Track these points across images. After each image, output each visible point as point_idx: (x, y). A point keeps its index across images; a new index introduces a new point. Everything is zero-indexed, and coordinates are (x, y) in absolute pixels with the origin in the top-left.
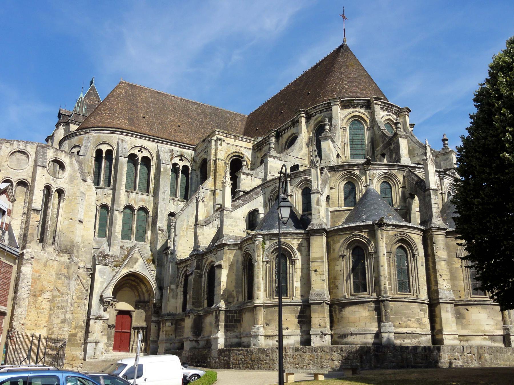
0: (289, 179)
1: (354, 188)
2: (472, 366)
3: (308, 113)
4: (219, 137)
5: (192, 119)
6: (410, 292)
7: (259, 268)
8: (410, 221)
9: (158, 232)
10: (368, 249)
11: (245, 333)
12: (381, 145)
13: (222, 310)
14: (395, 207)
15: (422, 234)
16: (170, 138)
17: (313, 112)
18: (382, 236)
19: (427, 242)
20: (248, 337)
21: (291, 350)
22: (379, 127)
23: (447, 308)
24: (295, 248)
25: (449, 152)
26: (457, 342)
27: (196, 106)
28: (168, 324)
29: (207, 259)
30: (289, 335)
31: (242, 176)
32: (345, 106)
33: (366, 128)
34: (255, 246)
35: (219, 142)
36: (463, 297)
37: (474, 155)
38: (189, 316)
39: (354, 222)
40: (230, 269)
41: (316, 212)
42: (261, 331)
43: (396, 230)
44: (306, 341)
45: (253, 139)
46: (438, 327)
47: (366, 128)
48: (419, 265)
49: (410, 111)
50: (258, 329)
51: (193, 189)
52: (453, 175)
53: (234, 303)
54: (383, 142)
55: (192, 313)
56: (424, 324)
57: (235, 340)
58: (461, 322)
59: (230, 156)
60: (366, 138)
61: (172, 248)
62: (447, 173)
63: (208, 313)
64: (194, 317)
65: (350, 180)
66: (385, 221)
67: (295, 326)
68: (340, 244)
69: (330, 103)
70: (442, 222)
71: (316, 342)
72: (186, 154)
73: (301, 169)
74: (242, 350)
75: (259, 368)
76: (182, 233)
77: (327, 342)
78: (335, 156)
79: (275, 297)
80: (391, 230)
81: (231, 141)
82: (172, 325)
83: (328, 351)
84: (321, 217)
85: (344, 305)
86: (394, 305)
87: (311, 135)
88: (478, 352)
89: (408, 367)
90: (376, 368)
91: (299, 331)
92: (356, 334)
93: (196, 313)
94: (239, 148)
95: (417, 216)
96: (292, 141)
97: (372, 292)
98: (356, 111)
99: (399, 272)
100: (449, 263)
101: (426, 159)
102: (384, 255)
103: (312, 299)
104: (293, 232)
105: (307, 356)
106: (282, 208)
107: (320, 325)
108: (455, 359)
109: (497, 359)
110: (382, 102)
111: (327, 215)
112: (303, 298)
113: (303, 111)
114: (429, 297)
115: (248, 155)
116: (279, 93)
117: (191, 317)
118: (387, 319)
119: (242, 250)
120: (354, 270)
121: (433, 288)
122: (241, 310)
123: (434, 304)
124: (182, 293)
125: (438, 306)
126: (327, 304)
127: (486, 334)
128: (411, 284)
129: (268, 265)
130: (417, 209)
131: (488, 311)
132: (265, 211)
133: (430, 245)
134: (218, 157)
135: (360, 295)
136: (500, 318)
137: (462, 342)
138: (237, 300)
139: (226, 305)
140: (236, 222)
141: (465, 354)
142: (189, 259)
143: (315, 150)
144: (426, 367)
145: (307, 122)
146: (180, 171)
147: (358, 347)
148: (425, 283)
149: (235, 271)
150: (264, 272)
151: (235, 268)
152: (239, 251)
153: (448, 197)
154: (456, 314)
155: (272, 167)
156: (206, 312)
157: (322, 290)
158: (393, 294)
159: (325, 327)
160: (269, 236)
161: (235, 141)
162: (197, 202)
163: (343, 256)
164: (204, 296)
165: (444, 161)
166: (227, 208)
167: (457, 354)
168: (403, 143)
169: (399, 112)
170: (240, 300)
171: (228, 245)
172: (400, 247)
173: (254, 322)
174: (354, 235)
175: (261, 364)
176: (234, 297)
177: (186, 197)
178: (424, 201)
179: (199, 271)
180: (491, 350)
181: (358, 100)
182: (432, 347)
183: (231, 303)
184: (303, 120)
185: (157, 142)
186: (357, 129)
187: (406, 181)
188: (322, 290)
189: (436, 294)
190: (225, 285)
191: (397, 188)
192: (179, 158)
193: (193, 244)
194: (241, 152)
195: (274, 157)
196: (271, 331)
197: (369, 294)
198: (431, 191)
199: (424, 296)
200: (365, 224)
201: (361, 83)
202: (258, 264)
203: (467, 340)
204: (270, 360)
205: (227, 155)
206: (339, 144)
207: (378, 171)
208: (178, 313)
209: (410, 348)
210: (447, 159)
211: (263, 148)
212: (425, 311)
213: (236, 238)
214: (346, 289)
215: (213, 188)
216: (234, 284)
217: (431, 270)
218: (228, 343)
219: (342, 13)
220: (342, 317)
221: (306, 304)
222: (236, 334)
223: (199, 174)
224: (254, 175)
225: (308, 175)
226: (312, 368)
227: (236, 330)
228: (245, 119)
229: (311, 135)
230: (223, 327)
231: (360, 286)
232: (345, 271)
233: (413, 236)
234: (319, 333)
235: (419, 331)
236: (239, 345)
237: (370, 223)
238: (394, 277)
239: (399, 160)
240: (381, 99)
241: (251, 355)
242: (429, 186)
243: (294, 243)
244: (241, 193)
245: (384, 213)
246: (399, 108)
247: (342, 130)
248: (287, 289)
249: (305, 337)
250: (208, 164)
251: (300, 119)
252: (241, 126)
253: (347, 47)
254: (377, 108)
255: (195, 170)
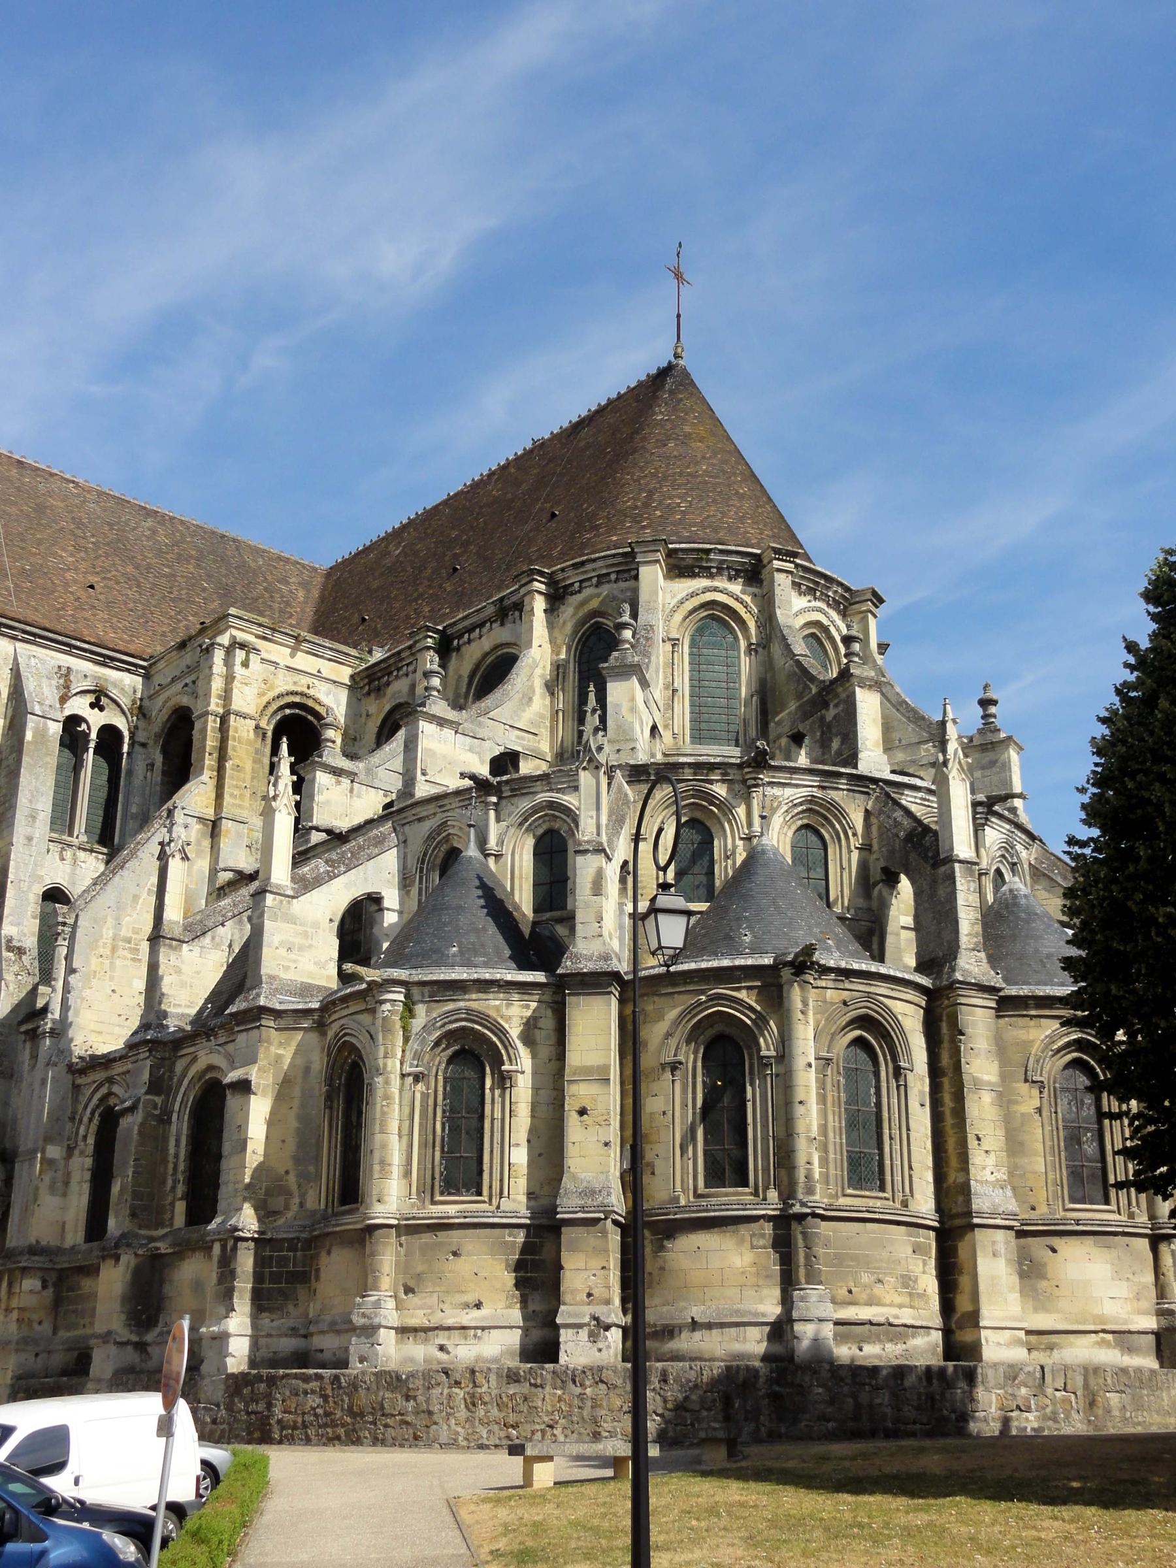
0: (494, 799)
1: (708, 842)
2: (1067, 1430)
3: (557, 582)
4: (241, 636)
5: (137, 567)
6: (882, 1188)
7: (387, 1097)
8: (881, 959)
9: (5, 954)
10: (758, 1044)
11: (328, 1318)
12: (793, 706)
13: (246, 1239)
14: (838, 909)
15: (923, 1004)
16: (59, 628)
17: (574, 578)
18: (805, 1003)
19: (939, 1029)
20: (338, 1332)
21: (493, 1378)
22: (788, 647)
23: (994, 1243)
24: (514, 1032)
25: (1002, 741)
26: (1019, 1354)
27: (150, 523)
28: (30, 1284)
29: (195, 1059)
30: (483, 1329)
31: (322, 778)
32: (680, 567)
33: (743, 644)
34: (379, 1022)
35: (240, 655)
36: (1043, 1209)
37: (1155, 768)
38: (117, 1258)
39: (715, 954)
40: (280, 1098)
41: (591, 917)
42: (389, 1314)
43: (848, 985)
44: (542, 1348)
45: (353, 652)
46: (963, 1304)
47: (743, 644)
48: (914, 1104)
49: (881, 601)
50: (377, 1305)
51: (134, 809)
52: (1011, 816)
53: (290, 1215)
54: (799, 696)
55: (129, 1245)
56: (923, 1296)
57: (288, 1345)
58: (1036, 1291)
59: (274, 706)
60: (744, 678)
61: (57, 1016)
62: (996, 808)
63: (185, 1248)
64: (133, 1261)
65: (698, 815)
66: (816, 957)
67: (503, 1296)
68: (665, 1026)
69: (632, 554)
70: (985, 966)
71: (576, 1351)
72: (115, 685)
73: (526, 768)
74: (319, 1377)
75: (377, 1441)
76: (94, 962)
77: (612, 1351)
78: (647, 732)
79: (438, 1198)
80: (831, 984)
81: (278, 652)
82: (44, 1287)
83: (619, 1382)
84: (605, 933)
85: (672, 1229)
86: (834, 1231)
87: (563, 656)
88: (1086, 1385)
89: (873, 1434)
90: (773, 1437)
91: (515, 1315)
92: (709, 1326)
93: (142, 1246)
94: (305, 680)
95: (903, 943)
96: (495, 672)
97: (766, 1188)
98: (716, 589)
99: (853, 1124)
100: (1005, 1100)
101: (945, 763)
102: (810, 1065)
103: (569, 1205)
104: (509, 978)
105: (548, 1397)
106: (660, 917)
107: (589, 1295)
108: (1019, 1408)
109: (1139, 1407)
110: (797, 566)
111: (621, 927)
112: (533, 1203)
113: (541, 574)
114: (939, 1209)
115: (334, 702)
116: (445, 503)
117: (124, 1259)
118: (813, 1277)
119: (323, 1034)
120: (707, 1111)
121: (953, 1177)
122: (317, 1237)
123: (953, 1230)
124: (88, 1175)
125: (968, 1237)
126: (615, 1222)
127: (1108, 1327)
128: (887, 1162)
129: (420, 1087)
130: (908, 920)
131: (1114, 1253)
132: (401, 903)
133: (946, 1038)
134: (237, 704)
135: (727, 1195)
136: (1150, 1278)
137: (1035, 1353)
138: (301, 1205)
139: (260, 1220)
140: (306, 935)
141: (1049, 1391)
142: (121, 1058)
143: (594, 711)
144: (930, 1435)
145: (550, 611)
146: (92, 745)
147: (717, 1368)
148: (929, 1162)
149: (296, 1103)
150: (407, 1110)
151: (297, 1092)
152: (314, 1037)
153: (996, 889)
154: (1020, 1264)
155: (431, 753)
156: (180, 1245)
157: (602, 1177)
158: (831, 1196)
159: (608, 1302)
160: (426, 990)
161: (292, 656)
162: (163, 857)
163: (674, 1067)
164: (173, 1188)
165: (983, 768)
166: (278, 886)
167: (1023, 1391)
168: (869, 707)
169: (848, 602)
170: (310, 1204)
171: (277, 1014)
172: (859, 1042)
173: (365, 1283)
174: (712, 998)
175: (386, 1426)
176: (289, 1193)
177: (110, 838)
178: (933, 894)
179: (158, 1100)
180: (1124, 1379)
181: (722, 552)
182: (950, 1369)
183: (275, 1213)
184: (539, 604)
185: (14, 638)
186: (714, 645)
187: (874, 829)
188: (602, 1177)
189: (961, 1199)
190: (261, 1150)
191: (844, 850)
192: (90, 698)
193: (141, 999)
194: (311, 692)
195: (441, 722)
196: (422, 1312)
197: (756, 1194)
198: (957, 865)
199: (924, 1203)
200: (750, 962)
201: (729, 499)
202: (387, 1082)
203: (1051, 1348)
204: (417, 1413)
205: (265, 699)
206: (658, 692)
207: (788, 791)
208: (69, 1242)
209: (885, 1372)
210: (993, 763)
211: (388, 684)
212: (926, 1253)
213: (305, 990)
214: (679, 1176)
215: (210, 813)
216: (291, 1146)
217: (949, 1121)
218: (263, 1353)
219: (672, 262)
220: (662, 1269)
221: (544, 1221)
222: (291, 1323)
223: (159, 758)
224: (362, 777)
225: (558, 791)
226: (561, 1438)
227: (291, 1308)
228: (319, 580)
229: (563, 656)
230: (248, 1296)
231: (727, 1168)
232: (677, 1114)
233: (898, 1007)
234: (587, 1320)
235: (906, 1316)
236: (302, 1359)
237: (767, 960)
238: (837, 1140)
239: (852, 759)
240: (795, 555)
241: (350, 1395)
242: (952, 849)
243: (513, 1014)
244: (316, 837)
245: (810, 928)
246: (847, 589)
247: (668, 646)
248: (480, 1172)
249: (537, 1335)
250: (198, 726)
251: (527, 599)
252: (304, 601)
253: (685, 374)
254: (782, 582)
255: (144, 745)
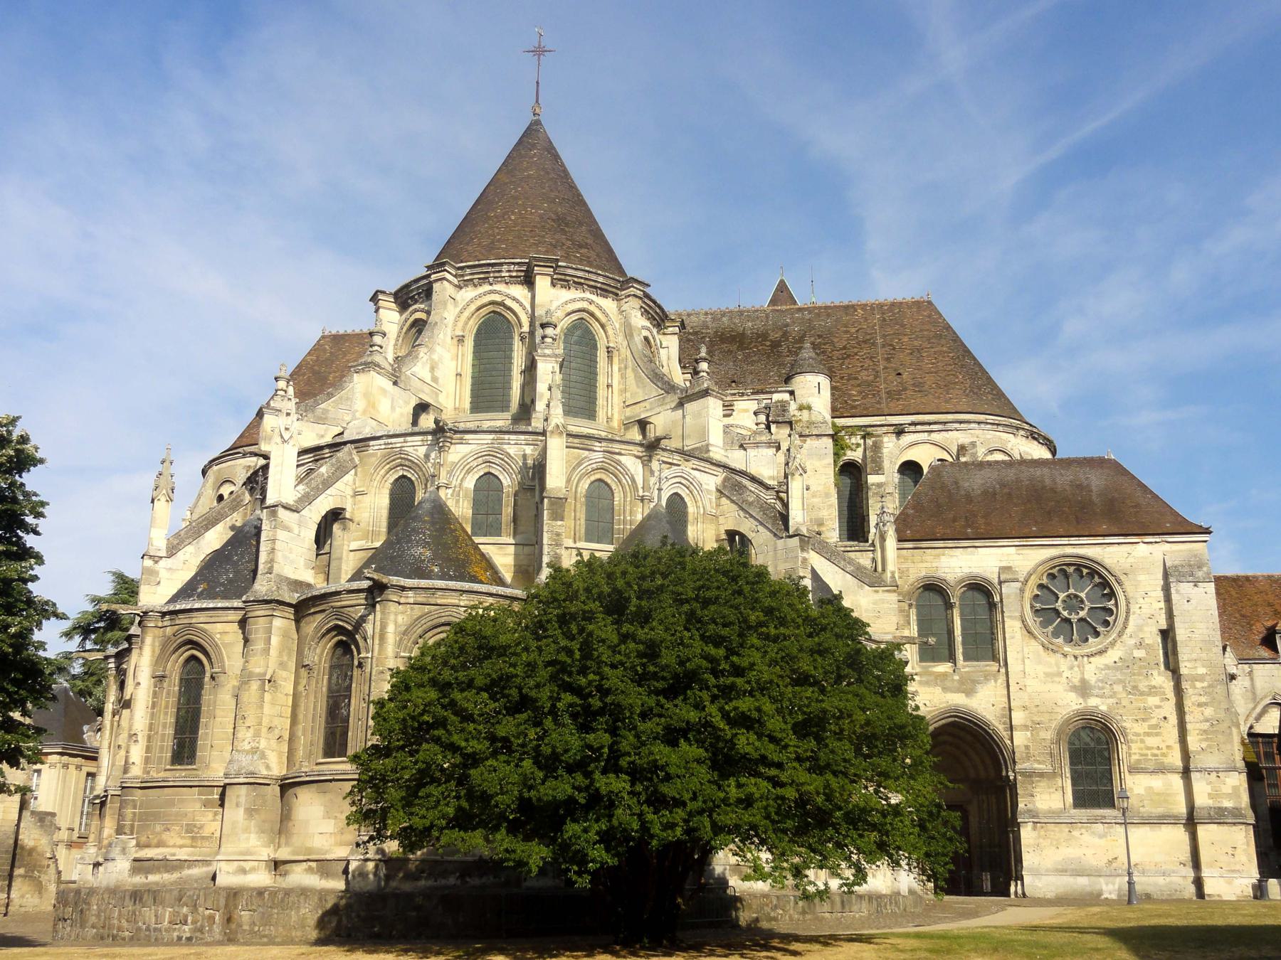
88: (226, 906)
131: (328, 796)
141: (201, 909)
235: (182, 854)
